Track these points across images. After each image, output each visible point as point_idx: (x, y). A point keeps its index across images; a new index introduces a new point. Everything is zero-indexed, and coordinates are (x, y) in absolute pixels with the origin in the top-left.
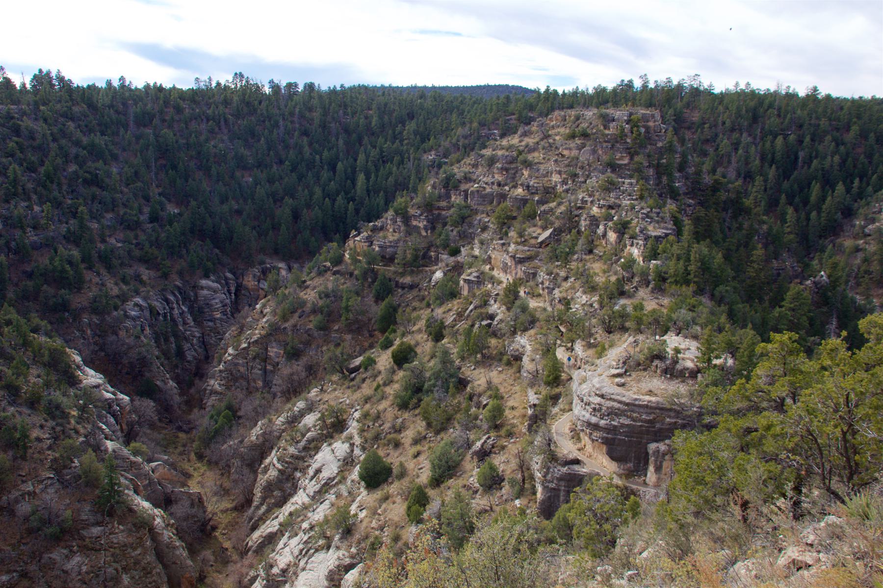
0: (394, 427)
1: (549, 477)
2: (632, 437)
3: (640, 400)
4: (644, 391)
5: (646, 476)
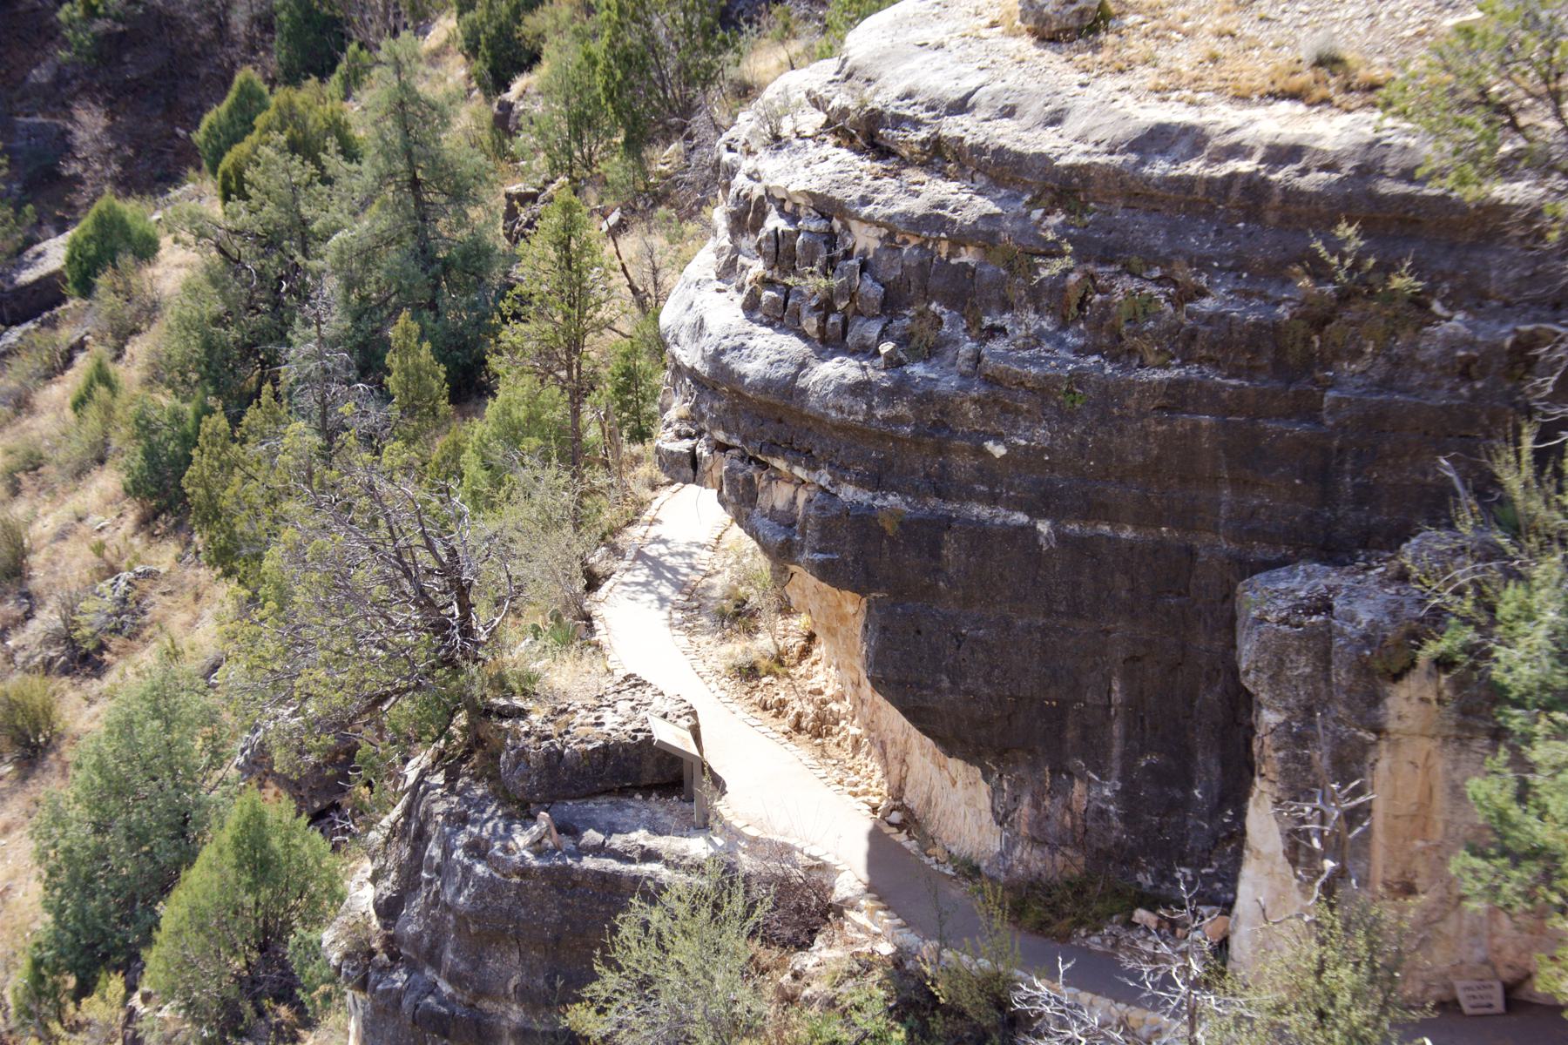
0: (65, 637)
1: (412, 923)
2: (1092, 510)
3: (1192, 140)
4: (1257, 69)
5: (1228, 907)
